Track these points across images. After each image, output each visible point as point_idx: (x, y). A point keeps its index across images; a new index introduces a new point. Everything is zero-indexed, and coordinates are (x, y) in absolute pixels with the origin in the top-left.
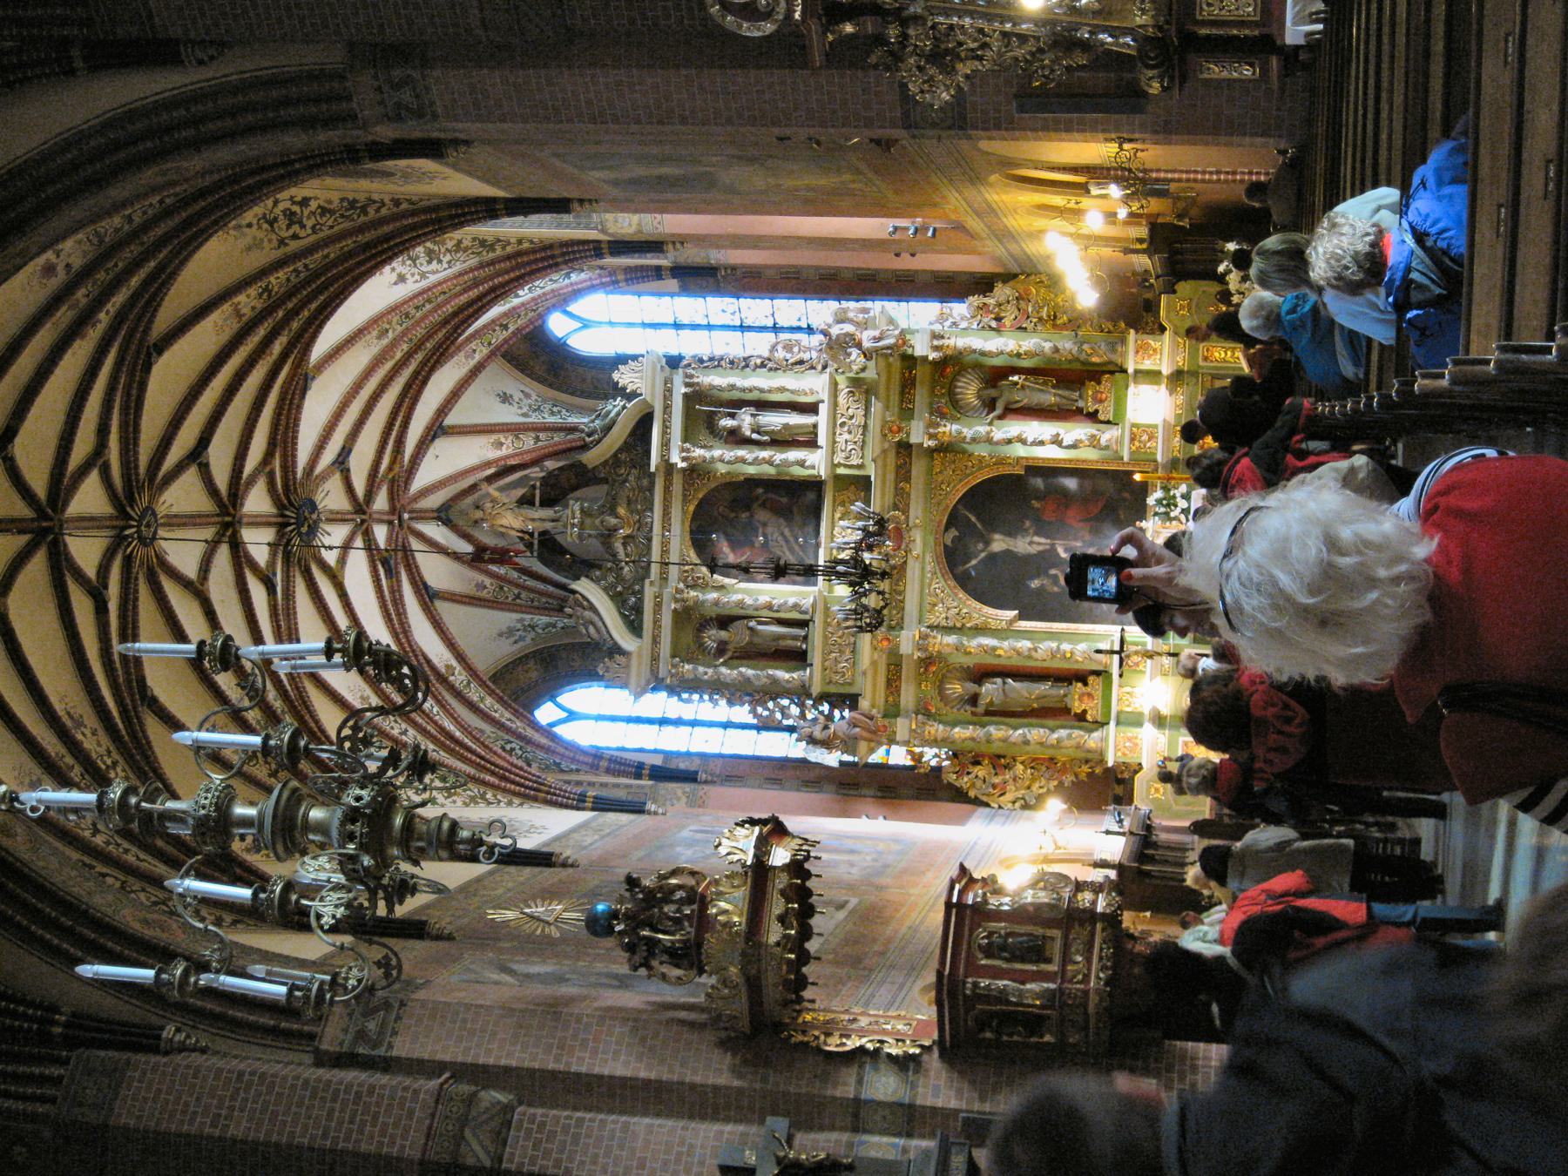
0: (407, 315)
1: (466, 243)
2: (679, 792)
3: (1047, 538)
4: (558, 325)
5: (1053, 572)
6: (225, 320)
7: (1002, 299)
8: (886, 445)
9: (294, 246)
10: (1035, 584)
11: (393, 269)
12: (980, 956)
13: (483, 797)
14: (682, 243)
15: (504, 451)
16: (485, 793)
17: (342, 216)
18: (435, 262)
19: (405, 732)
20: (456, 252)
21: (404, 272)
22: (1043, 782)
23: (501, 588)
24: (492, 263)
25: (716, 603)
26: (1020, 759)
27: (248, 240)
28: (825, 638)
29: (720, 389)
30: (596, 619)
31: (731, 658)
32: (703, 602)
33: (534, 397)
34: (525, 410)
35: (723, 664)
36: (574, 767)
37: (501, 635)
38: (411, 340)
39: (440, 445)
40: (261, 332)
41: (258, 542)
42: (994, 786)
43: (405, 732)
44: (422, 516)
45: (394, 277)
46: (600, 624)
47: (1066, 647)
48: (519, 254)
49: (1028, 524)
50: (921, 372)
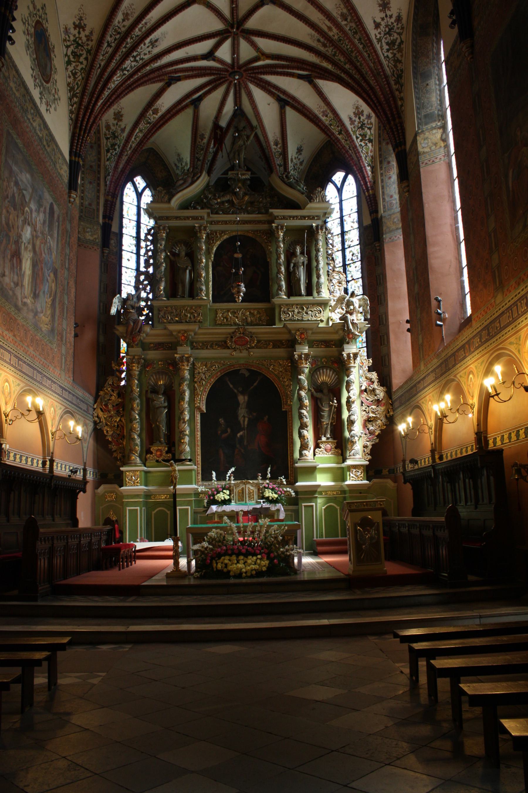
0: (356, 33)
1: (399, 66)
2: (96, 236)
3: (247, 425)
5: (229, 430)
7: (377, 392)
8: (293, 332)
10: (222, 421)
11: (383, 19)
13: (74, 96)
14: (408, 191)
16: (77, 97)
18: (387, 47)
20: (394, 60)
21: (382, 27)
22: (111, 433)
23: (202, 150)
24: (389, 84)
25: (201, 249)
26: (123, 419)
28: (184, 307)
29: (317, 244)
30: (187, 184)
31: (171, 260)
32: (200, 242)
33: (301, 167)
35: (167, 254)
36: (108, 183)
37: (179, 155)
38: (340, 40)
39: (275, 106)
42: (106, 405)
44: (237, 101)
45: (378, 20)
47: (187, 439)
49: (255, 414)
50: (334, 350)
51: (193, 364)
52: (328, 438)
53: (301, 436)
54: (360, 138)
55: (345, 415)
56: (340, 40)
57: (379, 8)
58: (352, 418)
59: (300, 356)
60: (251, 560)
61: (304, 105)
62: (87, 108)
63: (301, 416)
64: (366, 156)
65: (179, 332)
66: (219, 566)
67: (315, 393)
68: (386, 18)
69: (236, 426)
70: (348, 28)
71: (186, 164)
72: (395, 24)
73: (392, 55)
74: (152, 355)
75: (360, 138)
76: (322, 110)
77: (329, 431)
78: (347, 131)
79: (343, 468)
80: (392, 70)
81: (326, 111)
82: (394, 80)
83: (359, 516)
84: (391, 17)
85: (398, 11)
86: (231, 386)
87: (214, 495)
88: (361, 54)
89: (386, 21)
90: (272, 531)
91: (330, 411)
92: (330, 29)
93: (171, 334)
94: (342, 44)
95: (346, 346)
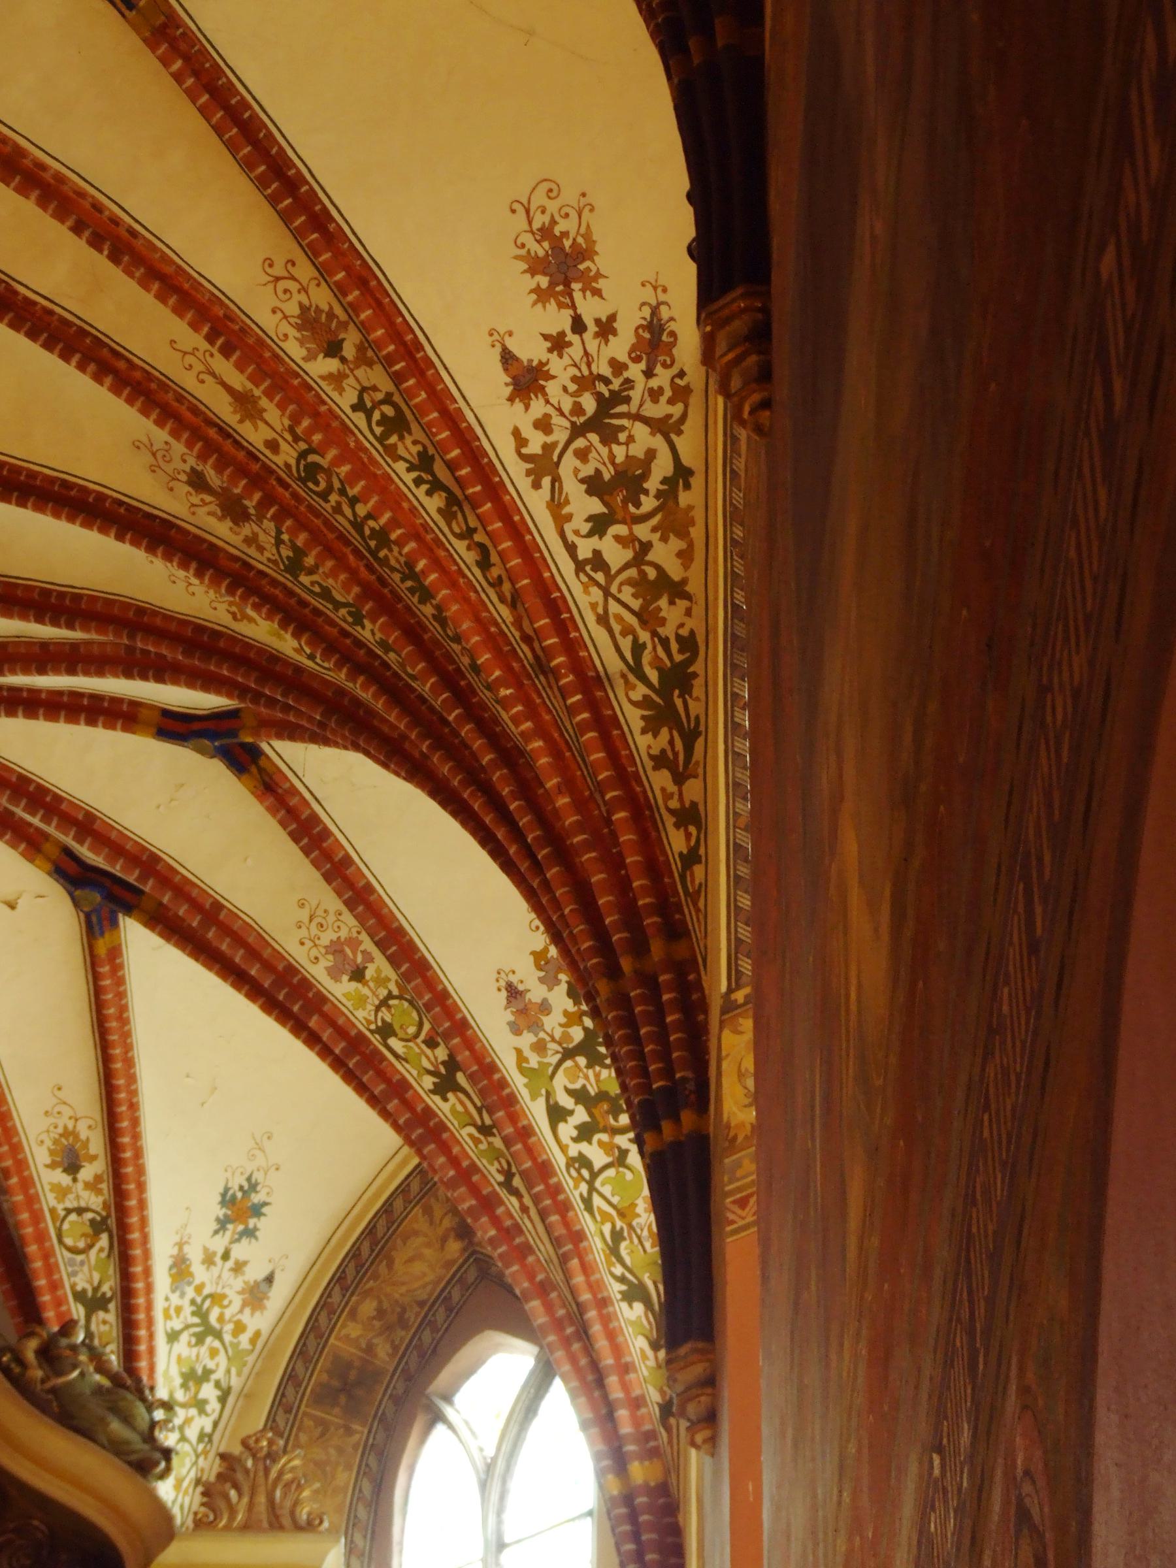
0: (397, 425)
11: (558, 344)
18: (596, 506)
20: (641, 585)
21: (552, 388)
33: (260, 1322)
34: (200, 1272)
38: (312, 471)
45: (531, 350)
54: (581, 1115)
56: (312, 471)
57: (531, 282)
61: (218, 906)
64: (617, 1236)
68: (571, 337)
70: (351, 397)
72: (635, 371)
73: (628, 554)
75: (581, 1115)
76: (327, 937)
78: (487, 1069)
80: (626, 644)
81: (354, 943)
82: (646, 703)
84: (606, 329)
85: (649, 295)
88: (431, 547)
89: (576, 352)
92: (242, 400)
94: (324, 496)
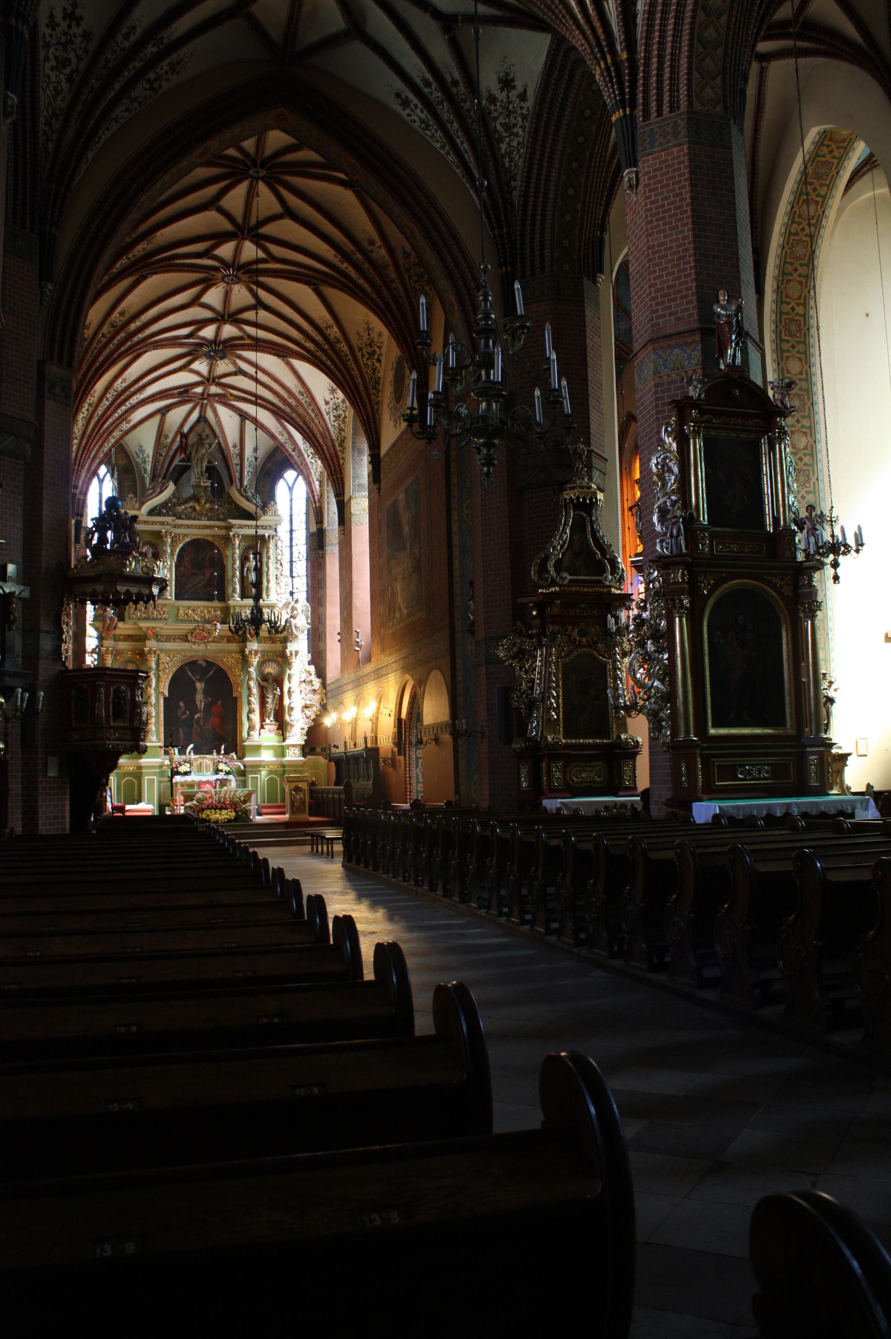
0: (310, 405)
1: (343, 434)
3: (204, 708)
4: (290, 475)
5: (188, 712)
6: (325, 321)
7: (314, 683)
9: (359, 355)
10: (182, 704)
11: (331, 399)
12: (115, 687)
14: (344, 534)
15: (232, 449)
17: (372, 378)
19: (107, 400)
20: (339, 429)
23: (166, 447)
24: (334, 446)
25: (165, 552)
27: (362, 333)
29: (268, 552)
30: (156, 493)
32: (166, 546)
37: (141, 446)
39: (236, 418)
40: (319, 338)
41: (208, 332)
43: (107, 400)
45: (328, 399)
46: (154, 495)
48: (337, 457)
49: (210, 699)
51: (159, 656)
52: (271, 721)
53: (249, 719)
54: (311, 456)
55: (286, 702)
58: (292, 705)
59: (250, 653)
60: (224, 812)
62: (85, 448)
63: (249, 703)
65: (148, 628)
66: (204, 816)
67: (261, 682)
69: (192, 707)
71: (148, 456)
74: (122, 645)
75: (311, 456)
77: (272, 715)
78: (300, 450)
79: (283, 746)
83: (294, 785)
84: (338, 398)
86: (190, 674)
87: (177, 768)
90: (237, 794)
91: (274, 698)
93: (140, 628)
95: (289, 644)
